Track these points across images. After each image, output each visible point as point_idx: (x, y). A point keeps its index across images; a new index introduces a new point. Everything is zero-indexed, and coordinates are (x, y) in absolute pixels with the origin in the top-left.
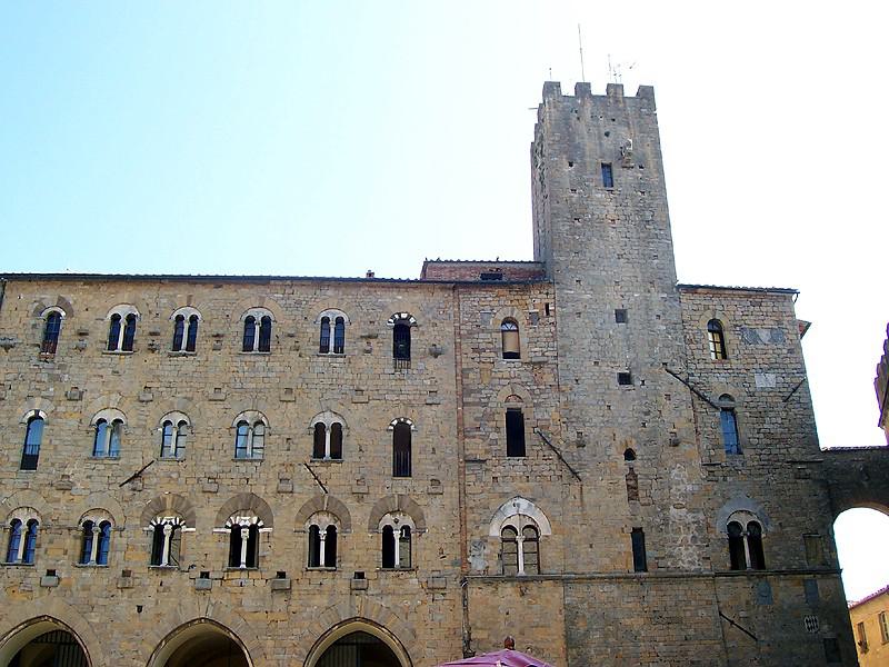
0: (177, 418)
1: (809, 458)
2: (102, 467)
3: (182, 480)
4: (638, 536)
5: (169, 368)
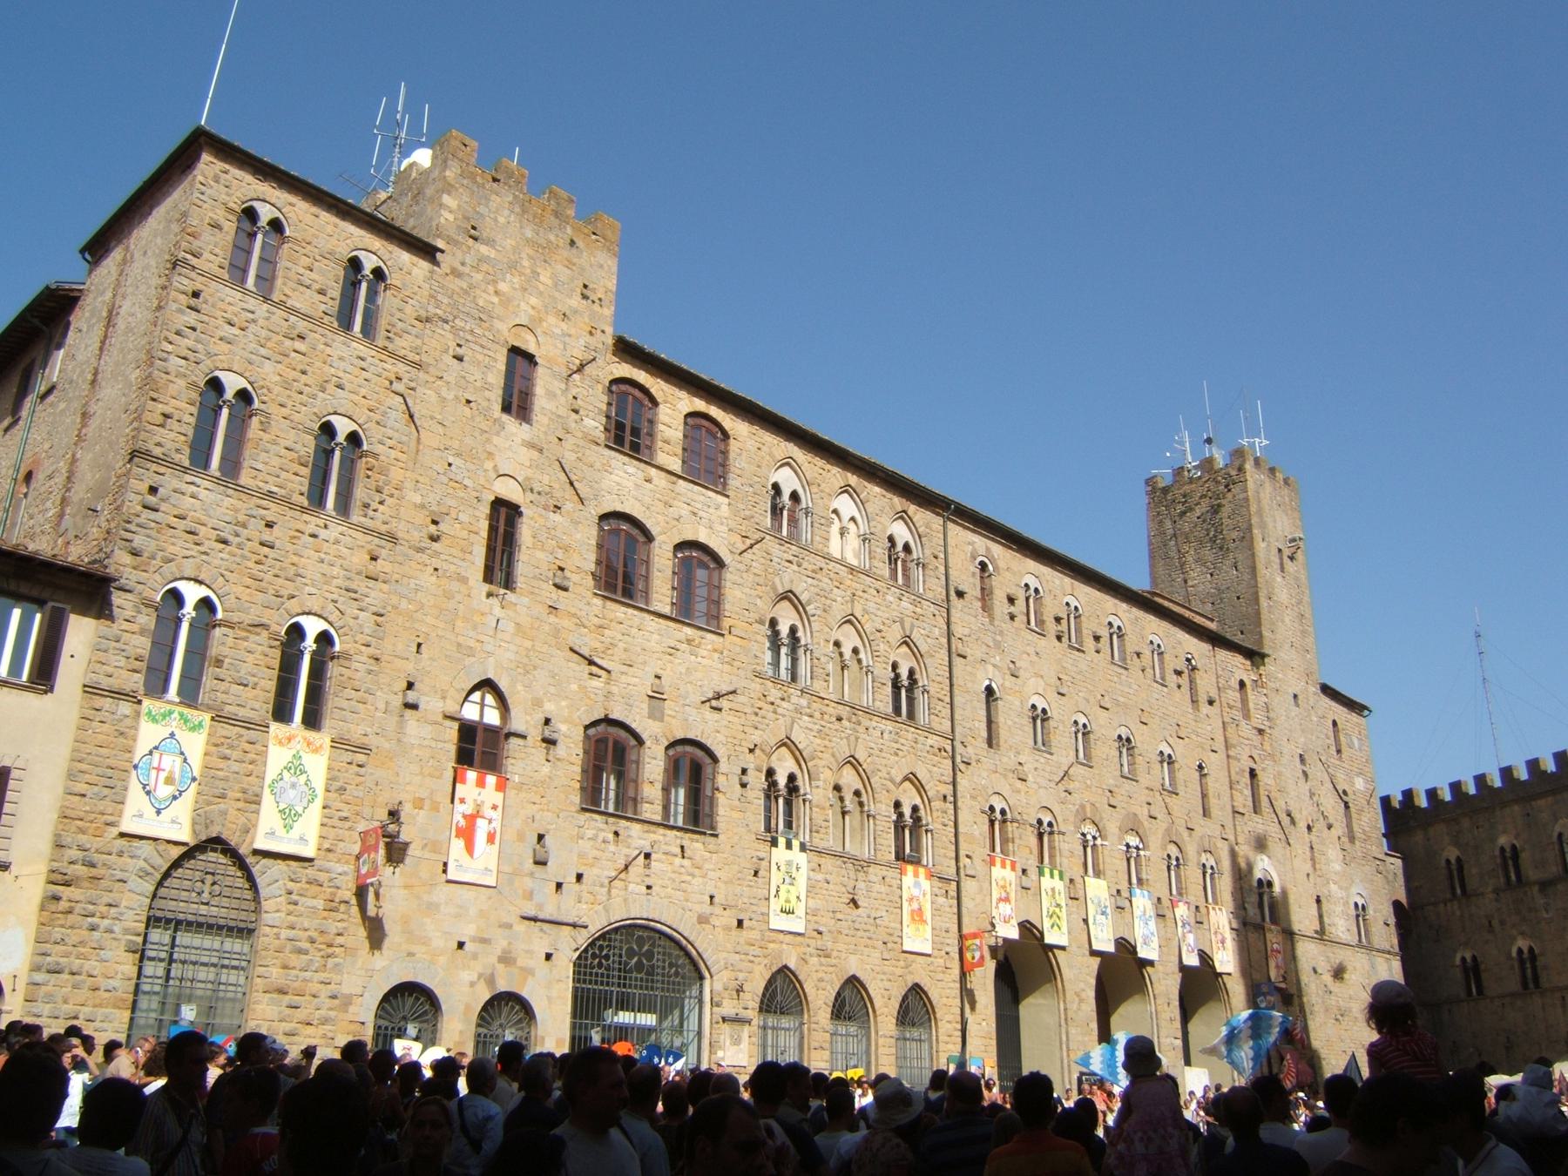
0: (1082, 720)
1: (1380, 856)
2: (1042, 760)
3: (1094, 789)
4: (1318, 901)
5: (1071, 661)
